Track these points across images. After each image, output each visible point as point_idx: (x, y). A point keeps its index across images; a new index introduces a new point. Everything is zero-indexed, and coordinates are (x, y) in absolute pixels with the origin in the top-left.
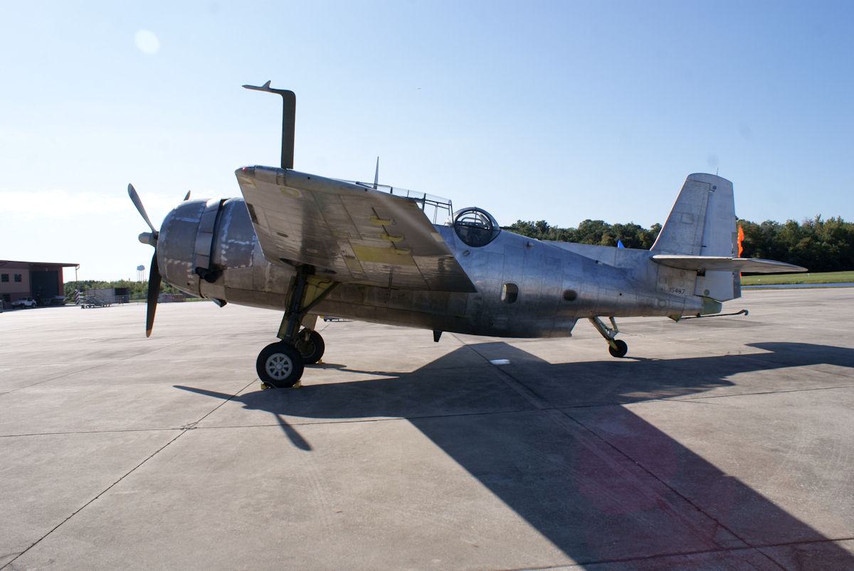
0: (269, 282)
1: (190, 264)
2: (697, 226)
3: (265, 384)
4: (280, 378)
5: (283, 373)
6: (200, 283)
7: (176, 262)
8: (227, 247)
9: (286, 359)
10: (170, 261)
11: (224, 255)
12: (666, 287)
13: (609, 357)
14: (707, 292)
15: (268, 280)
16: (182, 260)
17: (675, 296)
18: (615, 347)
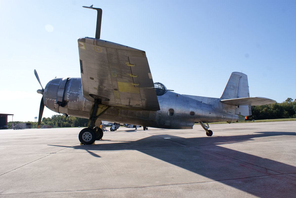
0: (84, 107)
1: (55, 100)
2: (236, 90)
3: (82, 143)
4: (87, 141)
5: (88, 139)
6: (59, 107)
7: (50, 99)
8: (69, 94)
9: (90, 134)
10: (48, 99)
11: (68, 97)
12: (226, 111)
13: (207, 136)
14: (240, 113)
15: (84, 106)
16: (53, 99)
17: (229, 114)
18: (208, 132)
